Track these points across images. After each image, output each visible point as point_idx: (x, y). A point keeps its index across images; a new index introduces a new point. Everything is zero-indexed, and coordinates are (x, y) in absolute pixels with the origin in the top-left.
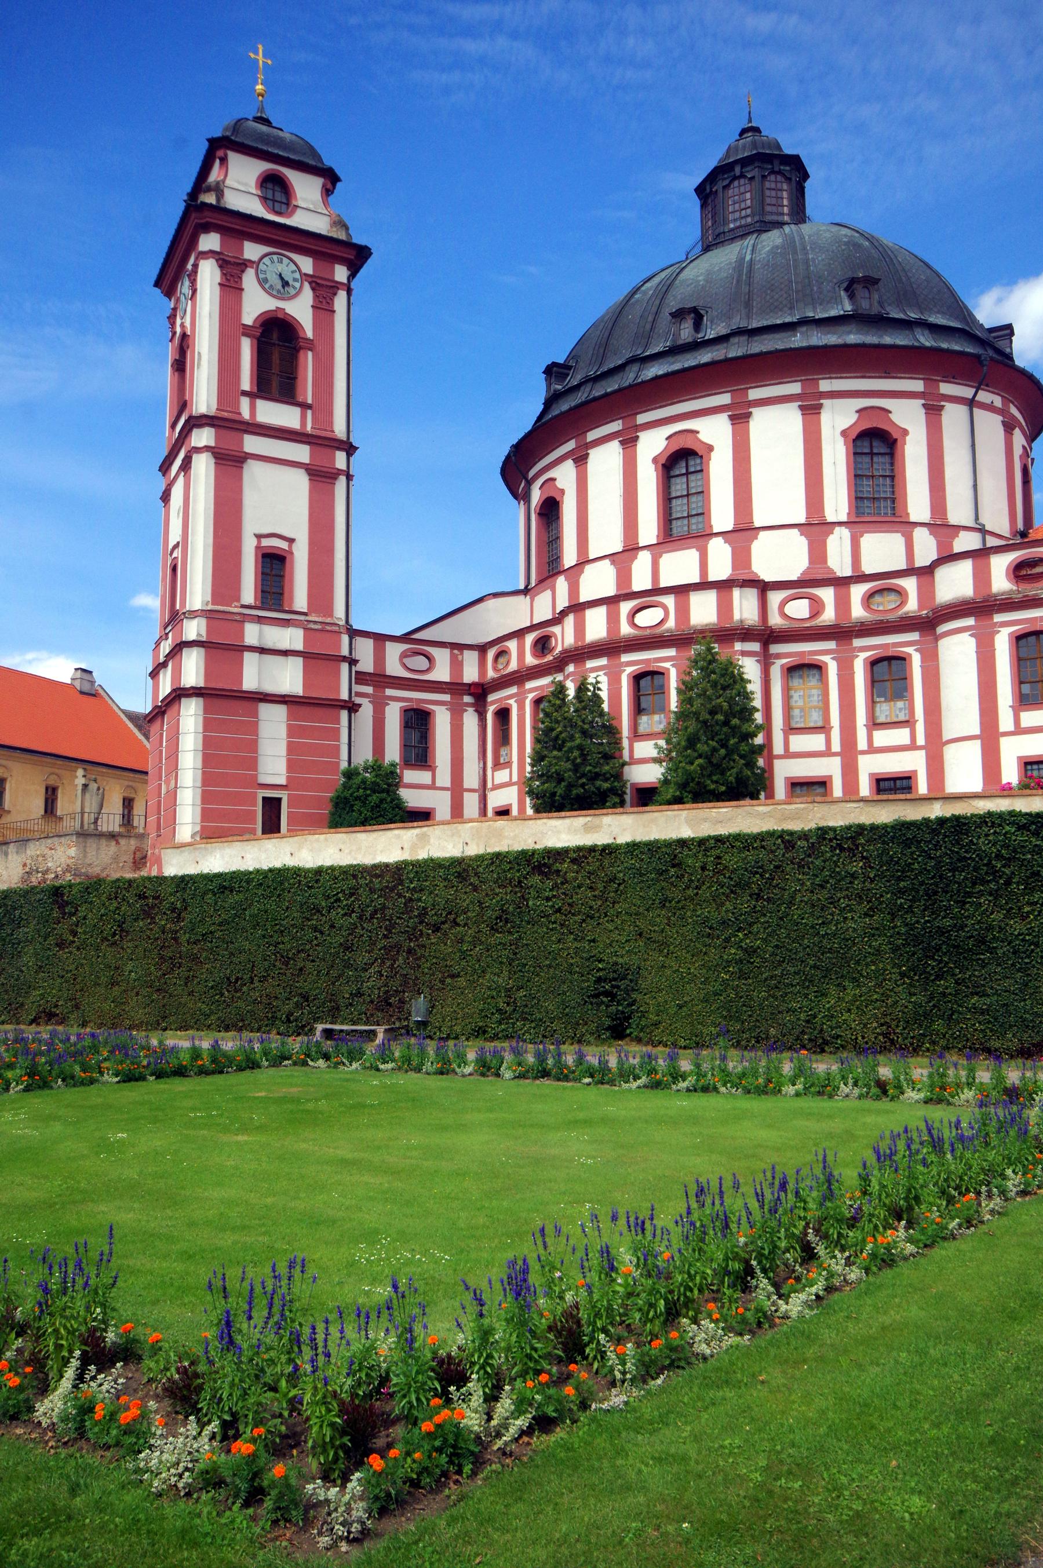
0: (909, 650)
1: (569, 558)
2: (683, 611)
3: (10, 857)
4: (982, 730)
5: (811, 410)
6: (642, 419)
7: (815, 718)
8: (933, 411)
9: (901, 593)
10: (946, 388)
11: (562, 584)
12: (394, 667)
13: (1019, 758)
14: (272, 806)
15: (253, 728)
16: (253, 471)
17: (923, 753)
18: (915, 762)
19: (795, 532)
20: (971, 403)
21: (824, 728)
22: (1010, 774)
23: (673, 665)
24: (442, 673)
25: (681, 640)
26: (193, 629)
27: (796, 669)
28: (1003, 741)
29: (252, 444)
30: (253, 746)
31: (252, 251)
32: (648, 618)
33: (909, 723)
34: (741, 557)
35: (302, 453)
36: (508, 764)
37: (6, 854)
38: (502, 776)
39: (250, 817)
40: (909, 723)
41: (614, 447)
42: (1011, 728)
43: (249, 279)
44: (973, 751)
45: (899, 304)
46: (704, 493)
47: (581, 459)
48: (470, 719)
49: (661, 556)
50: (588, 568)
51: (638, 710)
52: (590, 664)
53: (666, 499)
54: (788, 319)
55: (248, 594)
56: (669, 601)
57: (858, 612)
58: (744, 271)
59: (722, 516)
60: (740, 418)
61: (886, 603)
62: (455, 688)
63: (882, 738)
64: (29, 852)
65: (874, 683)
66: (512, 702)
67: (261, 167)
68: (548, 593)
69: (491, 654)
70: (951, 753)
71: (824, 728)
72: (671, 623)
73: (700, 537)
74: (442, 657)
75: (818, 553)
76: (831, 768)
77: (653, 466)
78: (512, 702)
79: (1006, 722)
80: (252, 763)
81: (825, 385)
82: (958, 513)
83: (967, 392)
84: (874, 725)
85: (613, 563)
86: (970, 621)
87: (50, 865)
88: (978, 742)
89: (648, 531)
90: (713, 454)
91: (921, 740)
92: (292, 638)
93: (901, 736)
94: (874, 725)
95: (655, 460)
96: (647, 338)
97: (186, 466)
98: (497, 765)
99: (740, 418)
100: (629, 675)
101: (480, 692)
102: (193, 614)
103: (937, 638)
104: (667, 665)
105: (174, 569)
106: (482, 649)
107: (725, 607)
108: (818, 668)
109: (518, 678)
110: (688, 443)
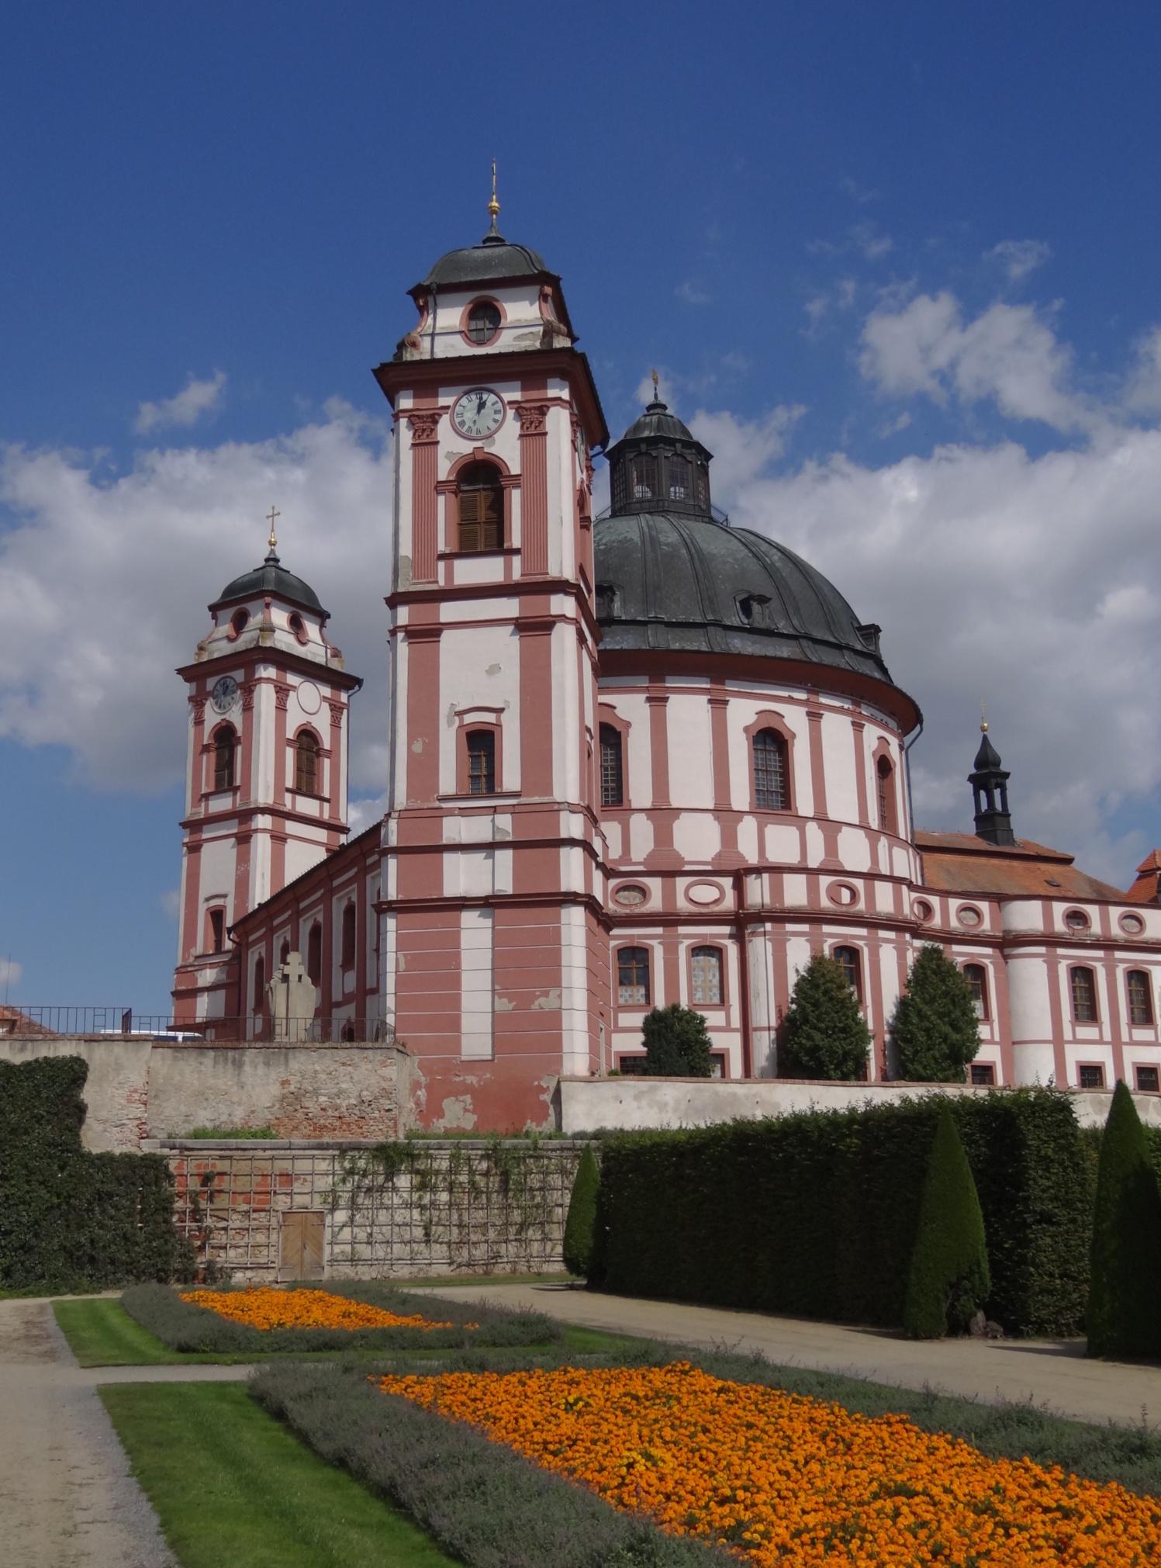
0: (987, 961)
3: (247, 1068)
4: (1054, 1037)
9: (978, 913)
13: (1077, 1062)
17: (997, 1048)
19: (861, 833)
23: (866, 944)
28: (1067, 1047)
37: (238, 1065)
42: (1071, 1039)
47: (658, 701)
49: (766, 826)
50: (684, 815)
52: (790, 927)
53: (758, 770)
54: (832, 639)
57: (954, 923)
59: (804, 803)
60: (814, 716)
64: (294, 1065)
66: (654, 943)
72: (861, 906)
77: (743, 736)
78: (654, 943)
85: (717, 818)
86: (1042, 950)
87: (344, 1086)
88: (1051, 1047)
89: (741, 796)
90: (796, 741)
91: (997, 1038)
95: (746, 729)
100: (830, 946)
102: (572, 809)
103: (1006, 957)
104: (861, 943)
110: (774, 723)
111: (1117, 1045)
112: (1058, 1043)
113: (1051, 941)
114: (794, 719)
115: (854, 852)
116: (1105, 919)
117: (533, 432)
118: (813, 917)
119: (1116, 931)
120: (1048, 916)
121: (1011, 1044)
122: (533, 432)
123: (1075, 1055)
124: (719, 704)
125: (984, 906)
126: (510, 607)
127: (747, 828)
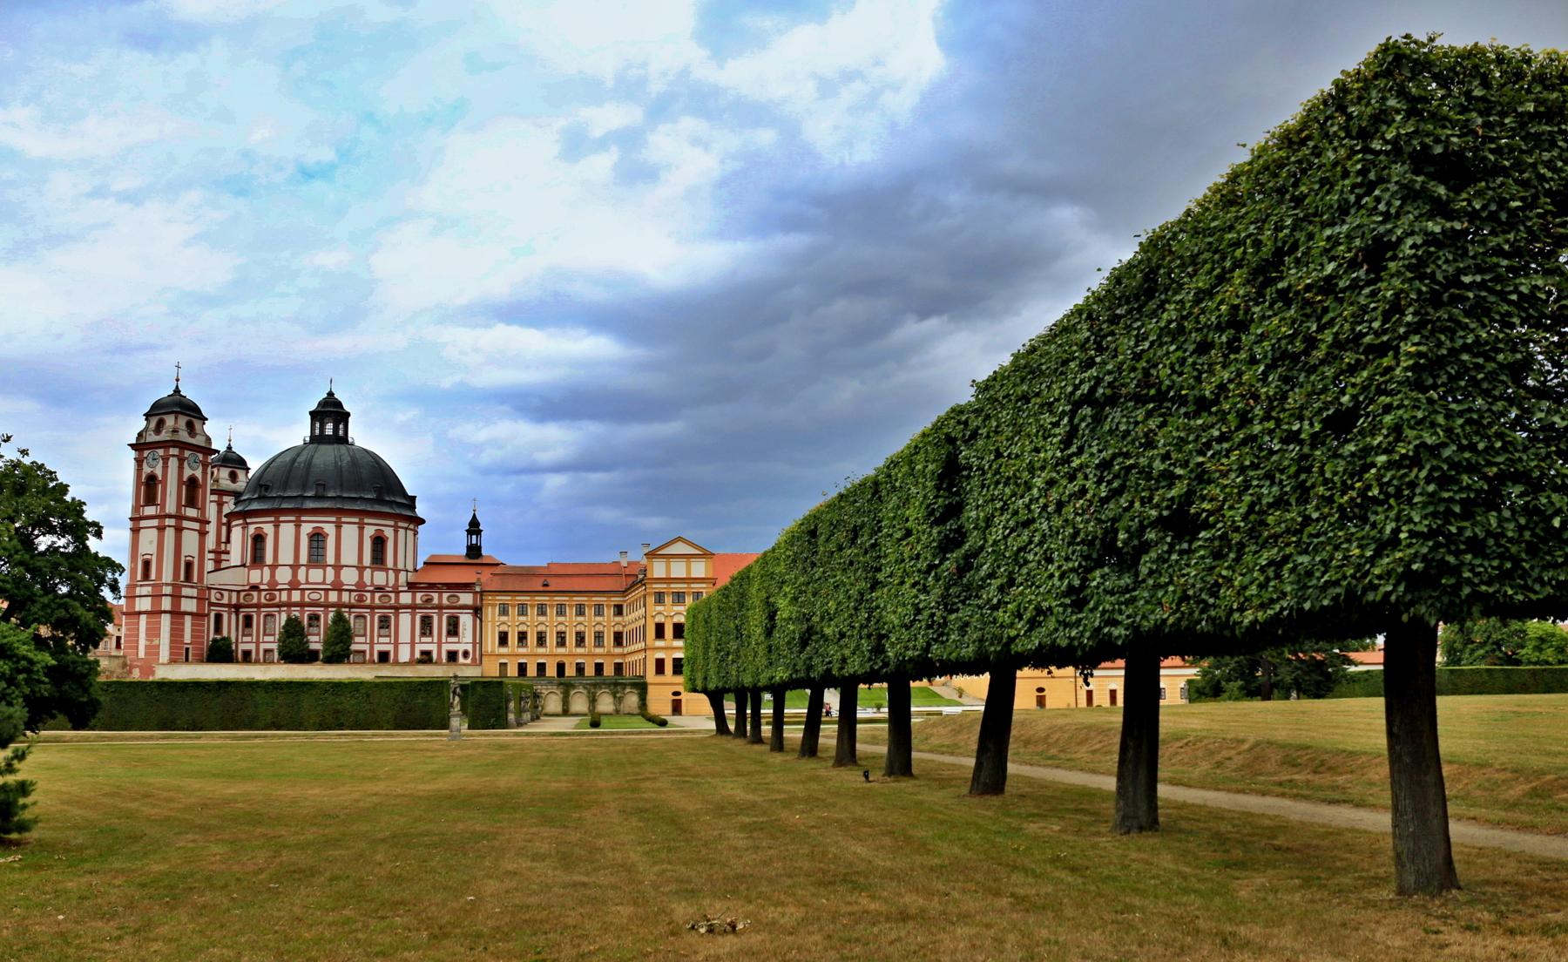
1: (269, 559)
2: (327, 596)
5: (361, 529)
6: (303, 518)
7: (362, 632)
8: (396, 532)
10: (400, 524)
11: (266, 570)
12: (213, 600)
14: (187, 649)
15: (183, 624)
16: (185, 532)
18: (390, 648)
20: (406, 529)
21: (365, 635)
22: (417, 655)
24: (225, 601)
25: (327, 606)
26: (166, 590)
27: (358, 617)
29: (185, 524)
30: (183, 630)
31: (187, 453)
32: (315, 596)
33: (389, 636)
34: (337, 575)
35: (196, 526)
36: (251, 635)
38: (249, 639)
39: (181, 654)
40: (389, 636)
41: (292, 525)
43: (186, 463)
44: (408, 647)
45: (388, 495)
46: (324, 548)
47: (277, 526)
48: (233, 617)
51: (310, 625)
55: (182, 578)
56: (322, 592)
58: (339, 470)
59: (330, 559)
60: (338, 527)
61: (386, 599)
62: (229, 606)
63: (381, 640)
65: (381, 621)
67: (187, 418)
68: (259, 571)
69: (242, 594)
70: (400, 646)
71: (365, 635)
73: (324, 566)
74: (226, 594)
75: (361, 576)
76: (366, 647)
79: (417, 640)
80: (182, 636)
81: (366, 521)
82: (400, 566)
83: (406, 525)
84: (379, 636)
92: (194, 592)
93: (387, 640)
94: (379, 636)
96: (304, 487)
97: (161, 529)
98: (243, 635)
99: (338, 527)
101: (237, 607)
102: (167, 584)
105: (147, 564)
106: (238, 592)
107: (340, 597)
108: (365, 617)
109: (258, 606)
111: (440, 644)
112: (413, 644)
113: (413, 607)
114: (329, 529)
115: (349, 577)
116: (440, 598)
117: (165, 467)
118: (302, 605)
119: (445, 602)
120: (414, 598)
121: (396, 644)
122: (165, 467)
123: (419, 648)
124: (298, 527)
125: (392, 595)
126: (155, 522)
127: (302, 572)
